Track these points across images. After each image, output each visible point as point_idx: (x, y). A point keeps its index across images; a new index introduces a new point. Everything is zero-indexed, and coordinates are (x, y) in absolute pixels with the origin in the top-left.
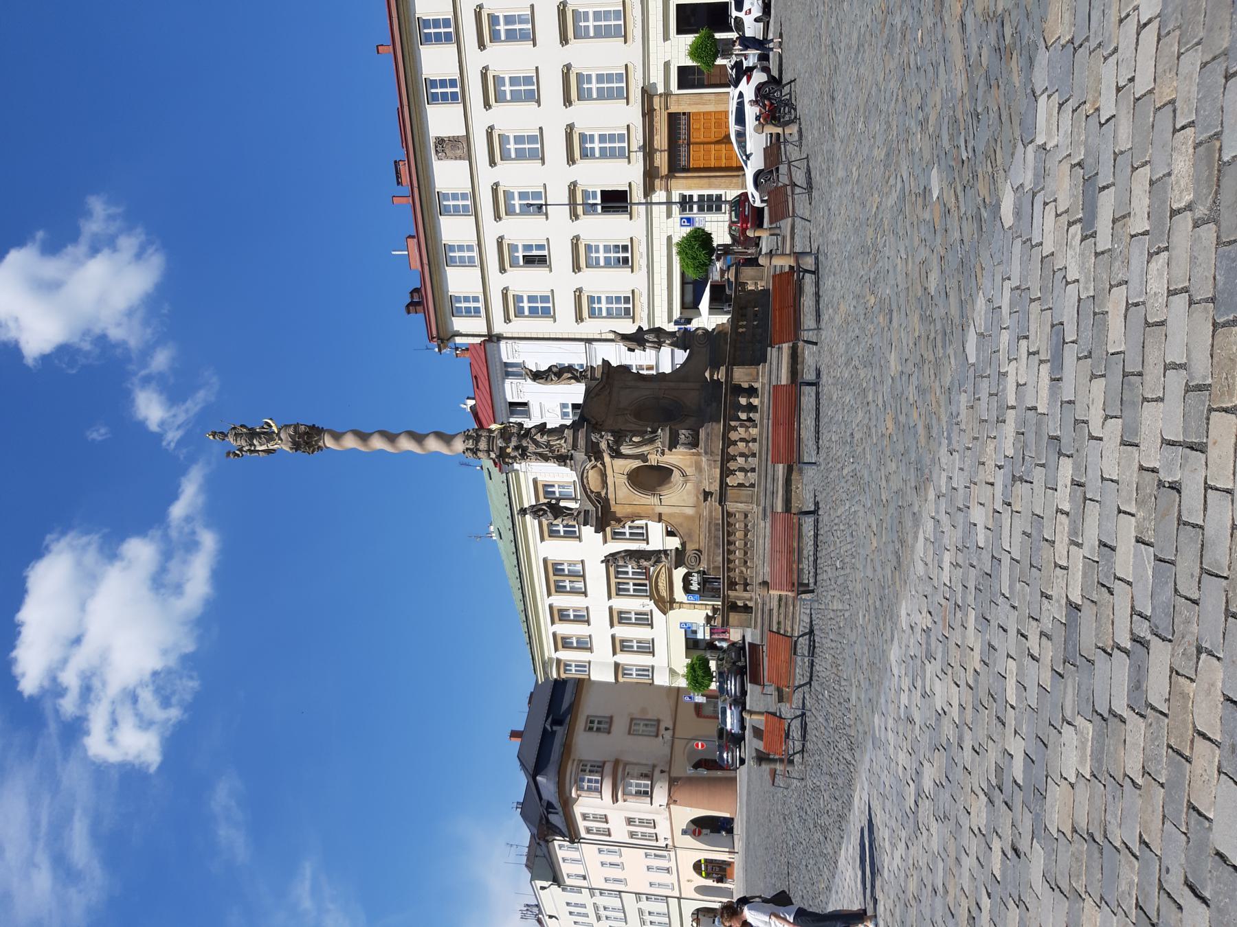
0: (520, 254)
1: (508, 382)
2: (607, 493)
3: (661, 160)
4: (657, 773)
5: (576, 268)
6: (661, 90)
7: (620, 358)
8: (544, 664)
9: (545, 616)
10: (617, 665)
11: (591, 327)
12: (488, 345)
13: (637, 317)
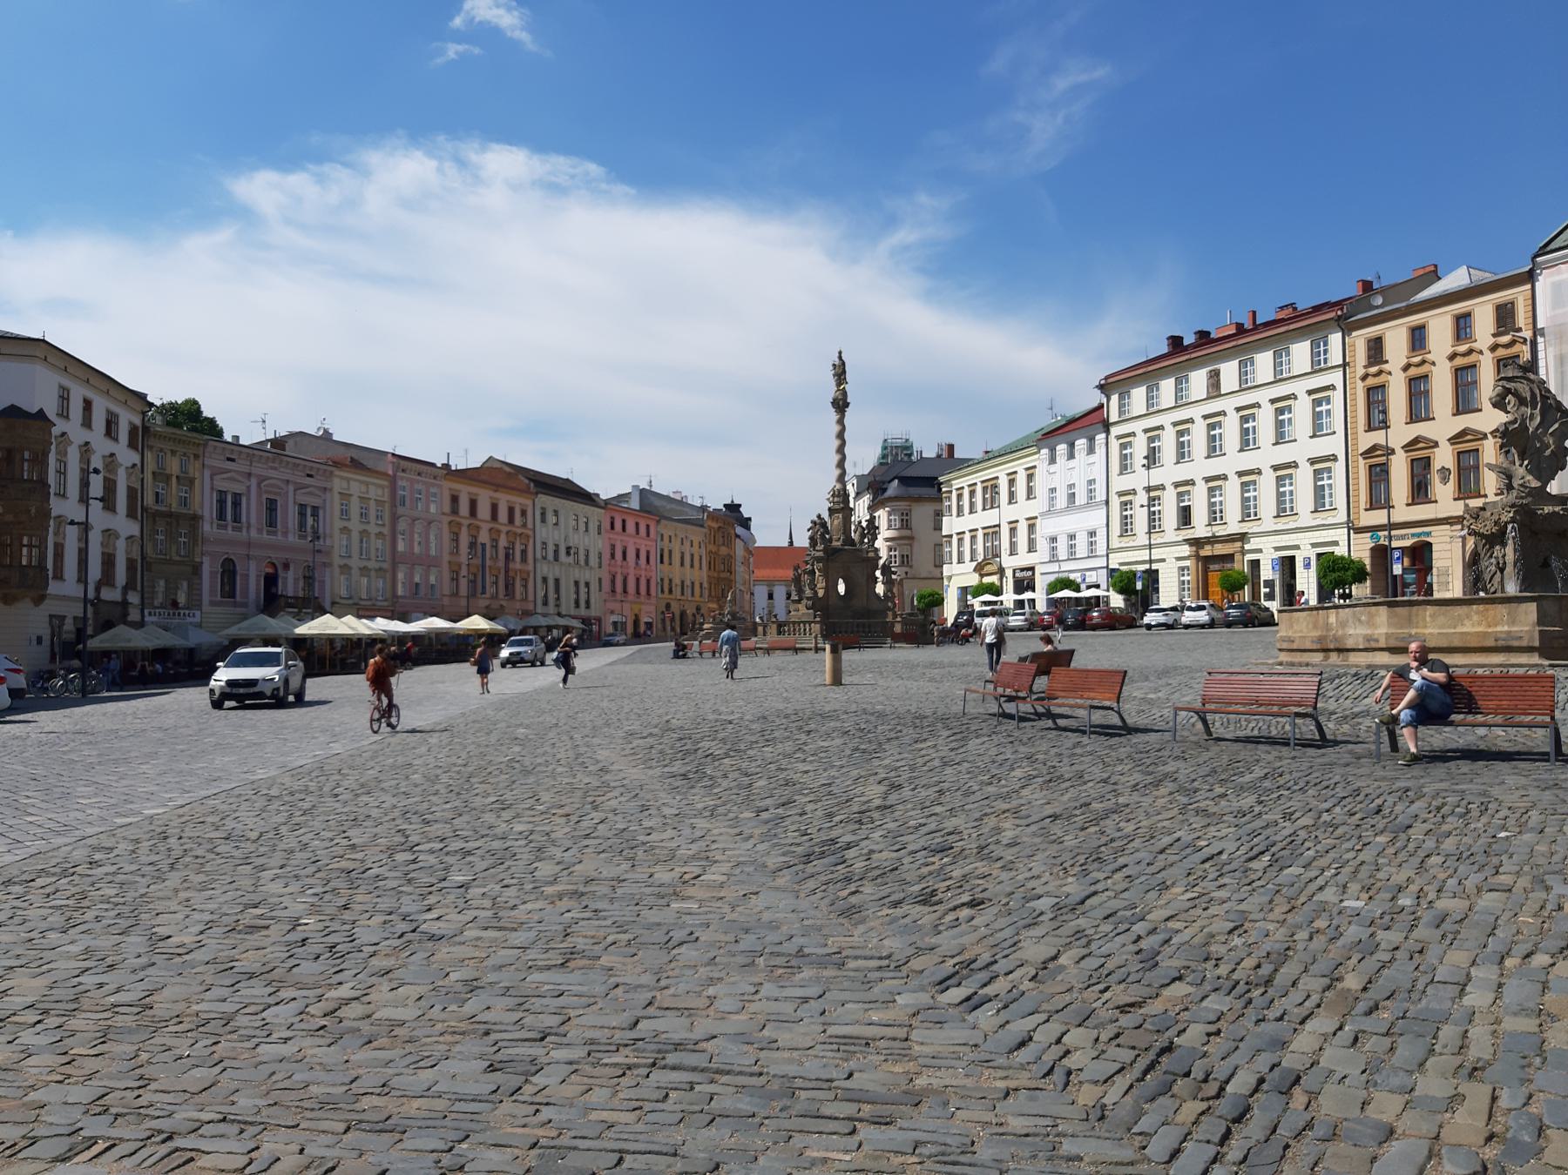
0: (1156, 444)
3: (1207, 551)
4: (905, 569)
6: (1247, 547)
8: (949, 481)
9: (1010, 468)
10: (951, 536)
11: (1115, 502)
12: (1100, 426)
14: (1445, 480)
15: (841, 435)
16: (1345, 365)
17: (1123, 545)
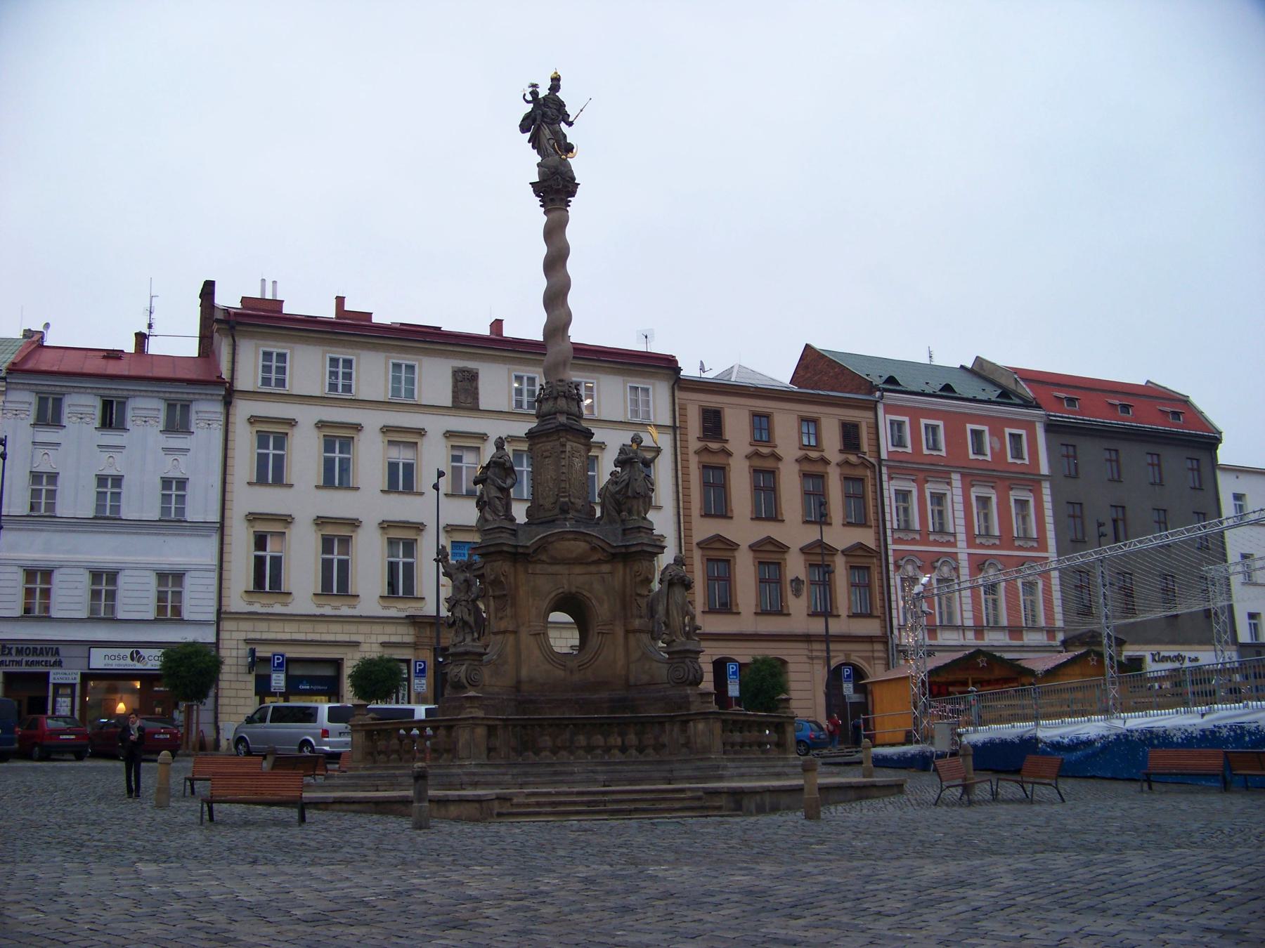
1: (162, 406)
2: (543, 562)
5: (321, 521)
7: (195, 570)
13: (254, 598)
14: (797, 593)
15: (556, 261)
16: (674, 428)
17: (256, 608)
